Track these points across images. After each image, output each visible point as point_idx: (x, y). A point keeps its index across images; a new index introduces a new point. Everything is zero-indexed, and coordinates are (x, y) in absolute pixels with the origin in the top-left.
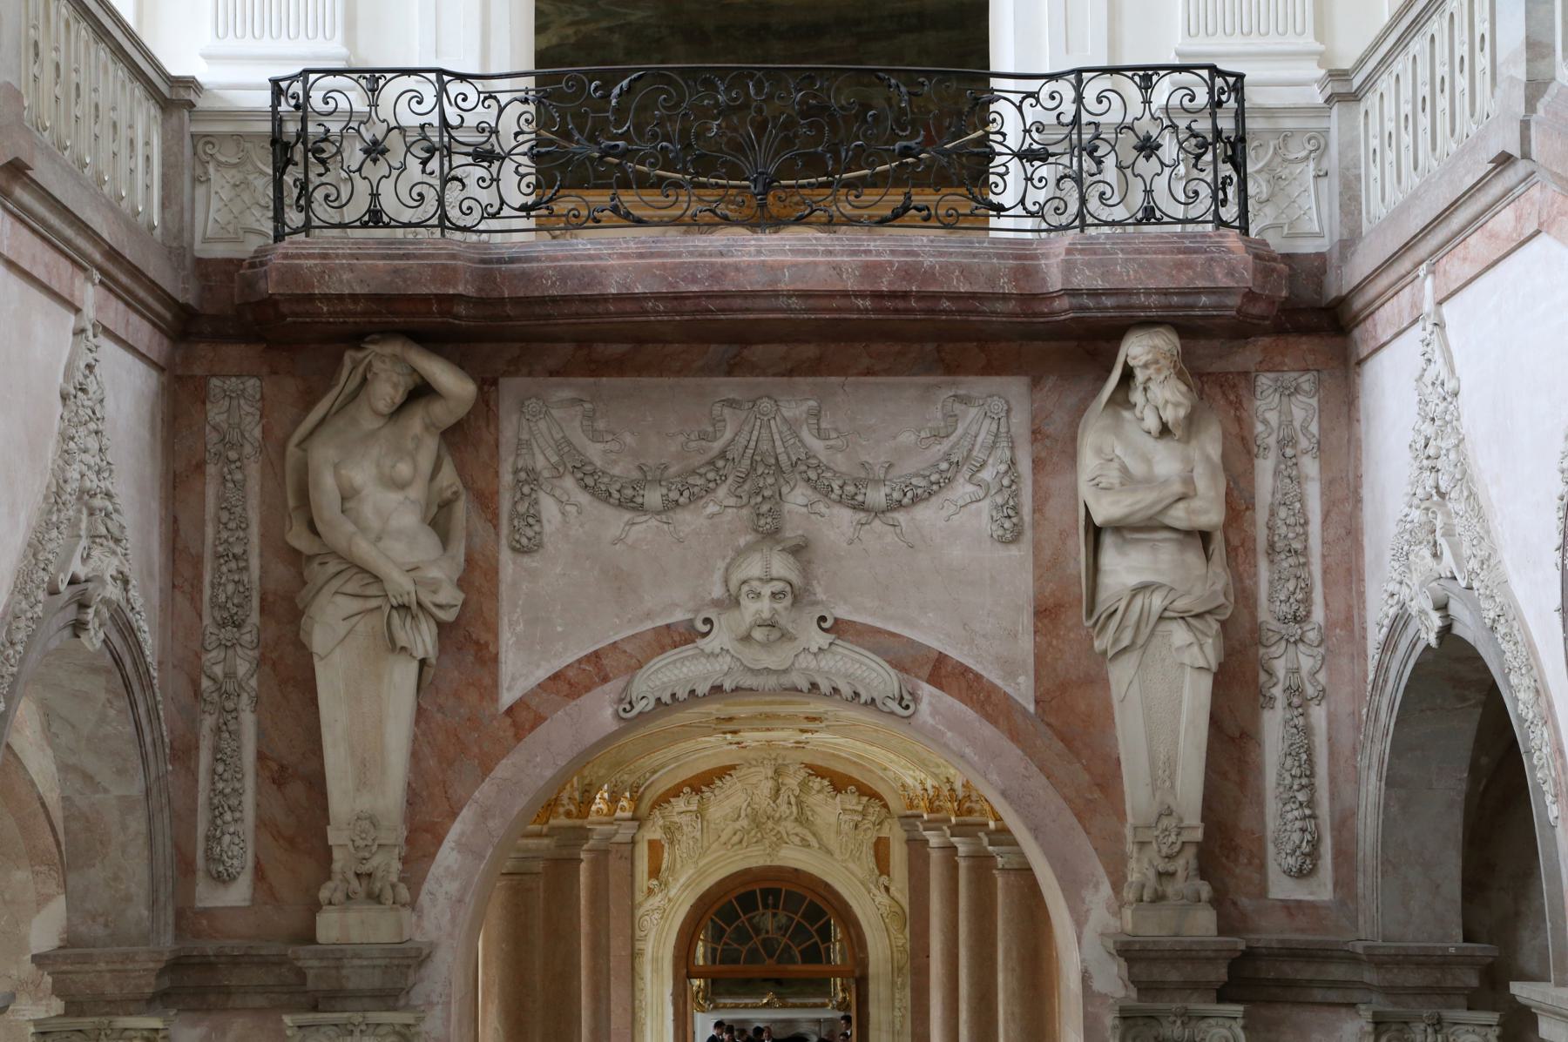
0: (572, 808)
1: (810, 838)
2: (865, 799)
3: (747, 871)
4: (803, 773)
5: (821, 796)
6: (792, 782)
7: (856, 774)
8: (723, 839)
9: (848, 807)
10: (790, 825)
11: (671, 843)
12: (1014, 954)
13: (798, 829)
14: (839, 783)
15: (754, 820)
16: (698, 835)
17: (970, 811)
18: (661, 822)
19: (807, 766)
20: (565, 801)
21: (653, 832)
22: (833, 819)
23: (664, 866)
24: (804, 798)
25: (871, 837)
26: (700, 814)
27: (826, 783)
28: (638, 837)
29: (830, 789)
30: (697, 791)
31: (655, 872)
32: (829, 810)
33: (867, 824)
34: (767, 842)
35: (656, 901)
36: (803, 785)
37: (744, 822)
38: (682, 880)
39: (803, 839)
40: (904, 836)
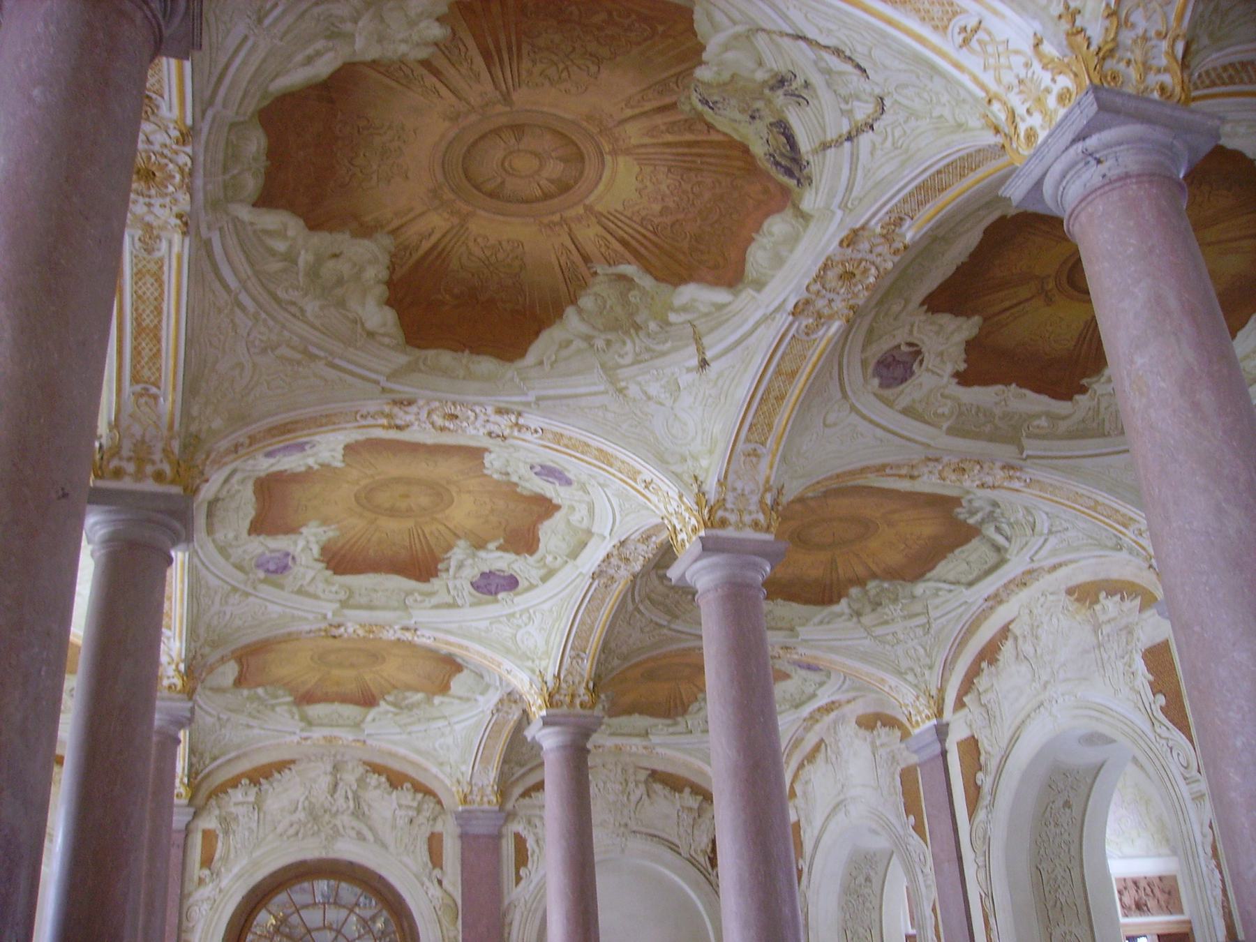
0: (167, 468)
1: (365, 831)
2: (420, 796)
3: (303, 863)
4: (361, 770)
5: (378, 792)
6: (350, 777)
7: (411, 771)
8: (280, 829)
9: (404, 802)
10: (346, 819)
11: (226, 833)
12: (1173, 303)
13: (355, 823)
14: (396, 780)
15: (311, 814)
16: (254, 825)
17: (723, 523)
18: (217, 812)
19: (365, 763)
20: (157, 456)
21: (209, 822)
22: (389, 814)
23: (217, 856)
24: (361, 793)
25: (425, 832)
26: (258, 805)
27: (383, 779)
28: (192, 826)
29: (387, 785)
30: (255, 782)
31: (207, 861)
32: (387, 806)
33: (421, 819)
34: (323, 835)
35: (207, 891)
36: (361, 781)
37: (301, 815)
38: (236, 870)
39: (359, 833)
40: (458, 830)
